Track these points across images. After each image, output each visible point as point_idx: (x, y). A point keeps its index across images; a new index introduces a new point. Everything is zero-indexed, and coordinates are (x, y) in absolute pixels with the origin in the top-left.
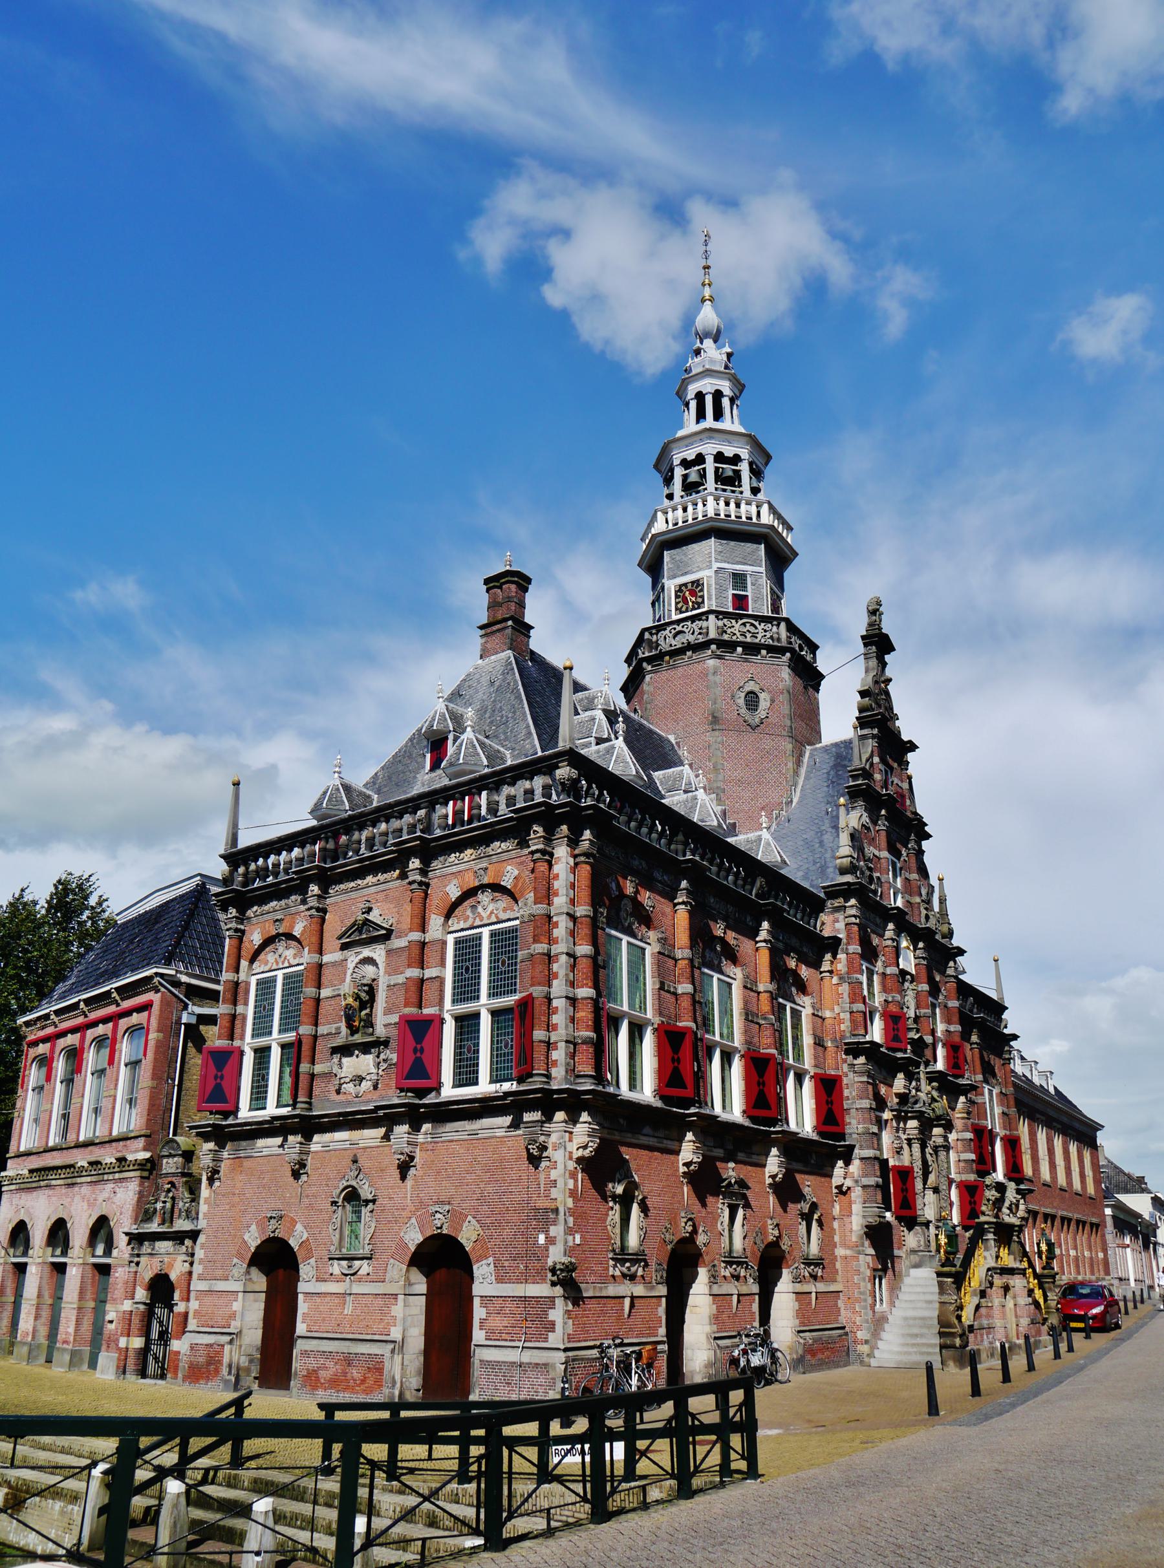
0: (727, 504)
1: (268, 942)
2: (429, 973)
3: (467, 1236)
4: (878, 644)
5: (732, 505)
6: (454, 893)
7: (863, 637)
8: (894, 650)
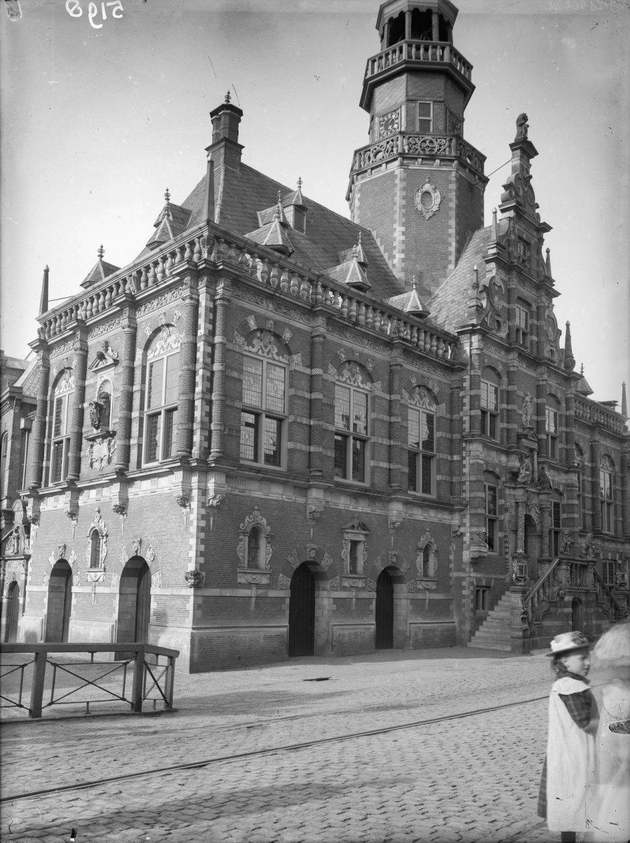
0: (418, 48)
1: (61, 373)
3: (148, 558)
4: (524, 148)
5: (422, 51)
6: (149, 333)
7: (511, 146)
8: (536, 154)
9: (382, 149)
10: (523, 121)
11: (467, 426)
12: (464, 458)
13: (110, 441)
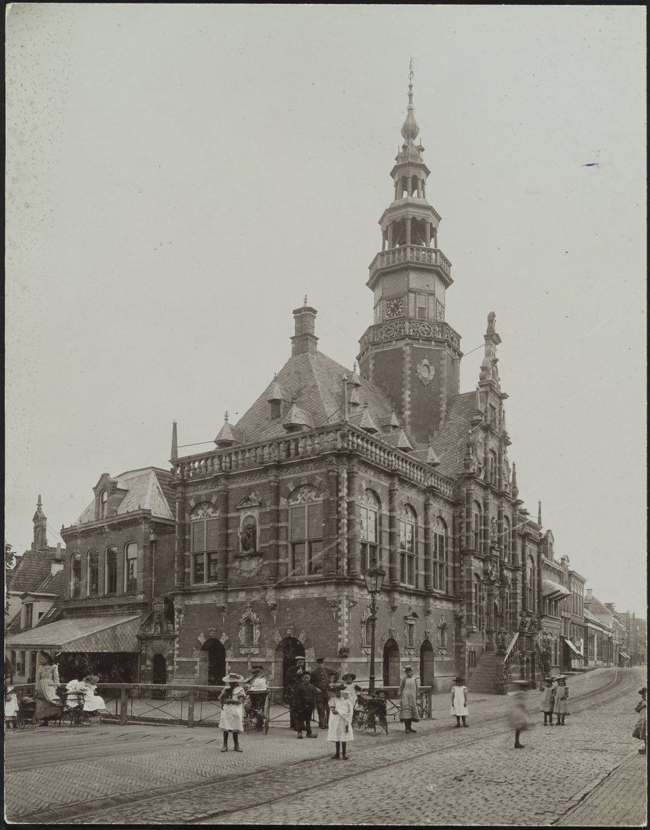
2: (282, 524)
3: (301, 638)
4: (492, 338)
7: (485, 336)
9: (391, 328)
10: (491, 318)
11: (464, 543)
12: (461, 565)
13: (259, 559)
